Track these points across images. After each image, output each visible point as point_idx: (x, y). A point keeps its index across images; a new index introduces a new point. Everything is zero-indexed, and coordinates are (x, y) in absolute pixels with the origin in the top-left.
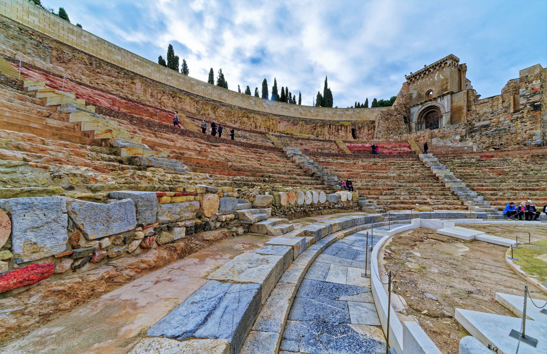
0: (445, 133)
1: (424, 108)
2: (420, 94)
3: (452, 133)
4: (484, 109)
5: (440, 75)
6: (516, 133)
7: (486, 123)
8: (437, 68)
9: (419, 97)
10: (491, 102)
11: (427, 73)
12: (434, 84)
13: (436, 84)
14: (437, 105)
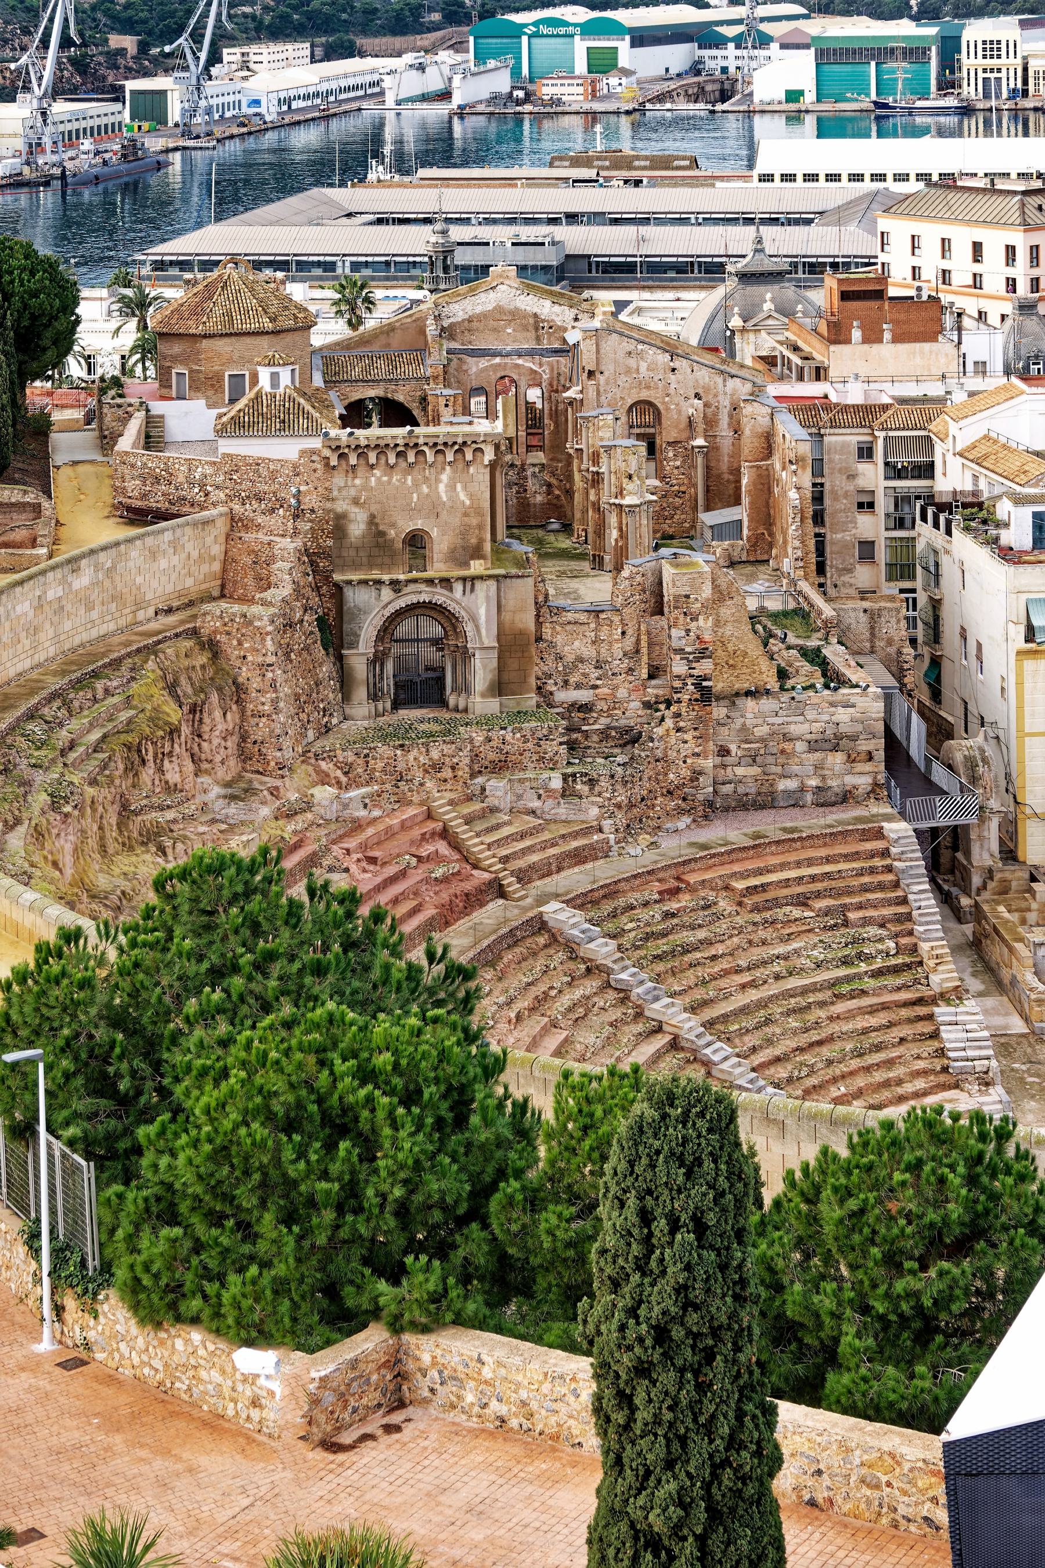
0: (507, 748)
1: (402, 603)
2: (382, 534)
3: (527, 754)
4: (577, 643)
5: (459, 486)
6: (664, 759)
7: (583, 696)
8: (450, 456)
9: (378, 545)
10: (593, 626)
11: (411, 457)
12: (435, 510)
13: (444, 515)
14: (452, 607)
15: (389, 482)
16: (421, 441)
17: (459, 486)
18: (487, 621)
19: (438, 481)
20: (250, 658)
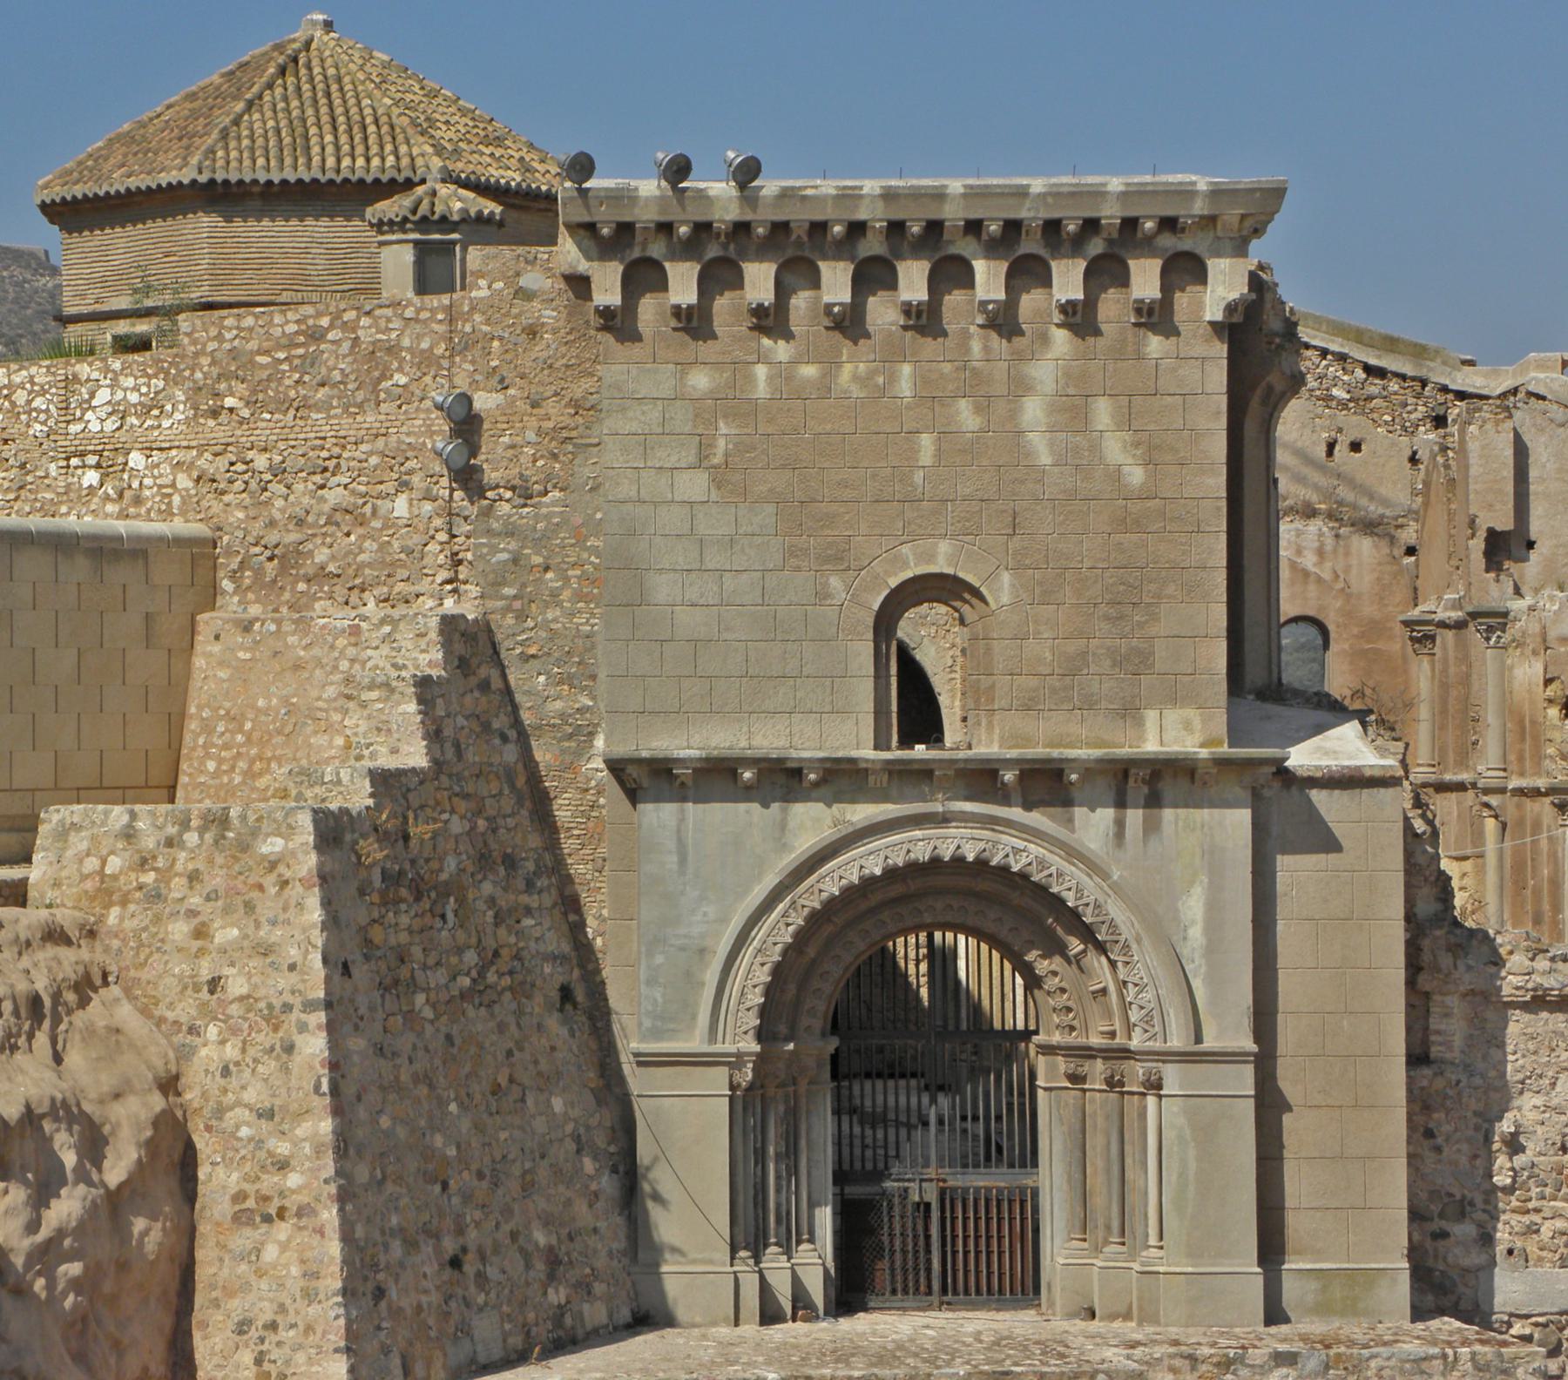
5: (1103, 412)
14: (1072, 885)
15: (825, 386)
16: (953, 214)
17: (1103, 412)
18: (1213, 947)
19: (1020, 387)
20: (237, 986)
